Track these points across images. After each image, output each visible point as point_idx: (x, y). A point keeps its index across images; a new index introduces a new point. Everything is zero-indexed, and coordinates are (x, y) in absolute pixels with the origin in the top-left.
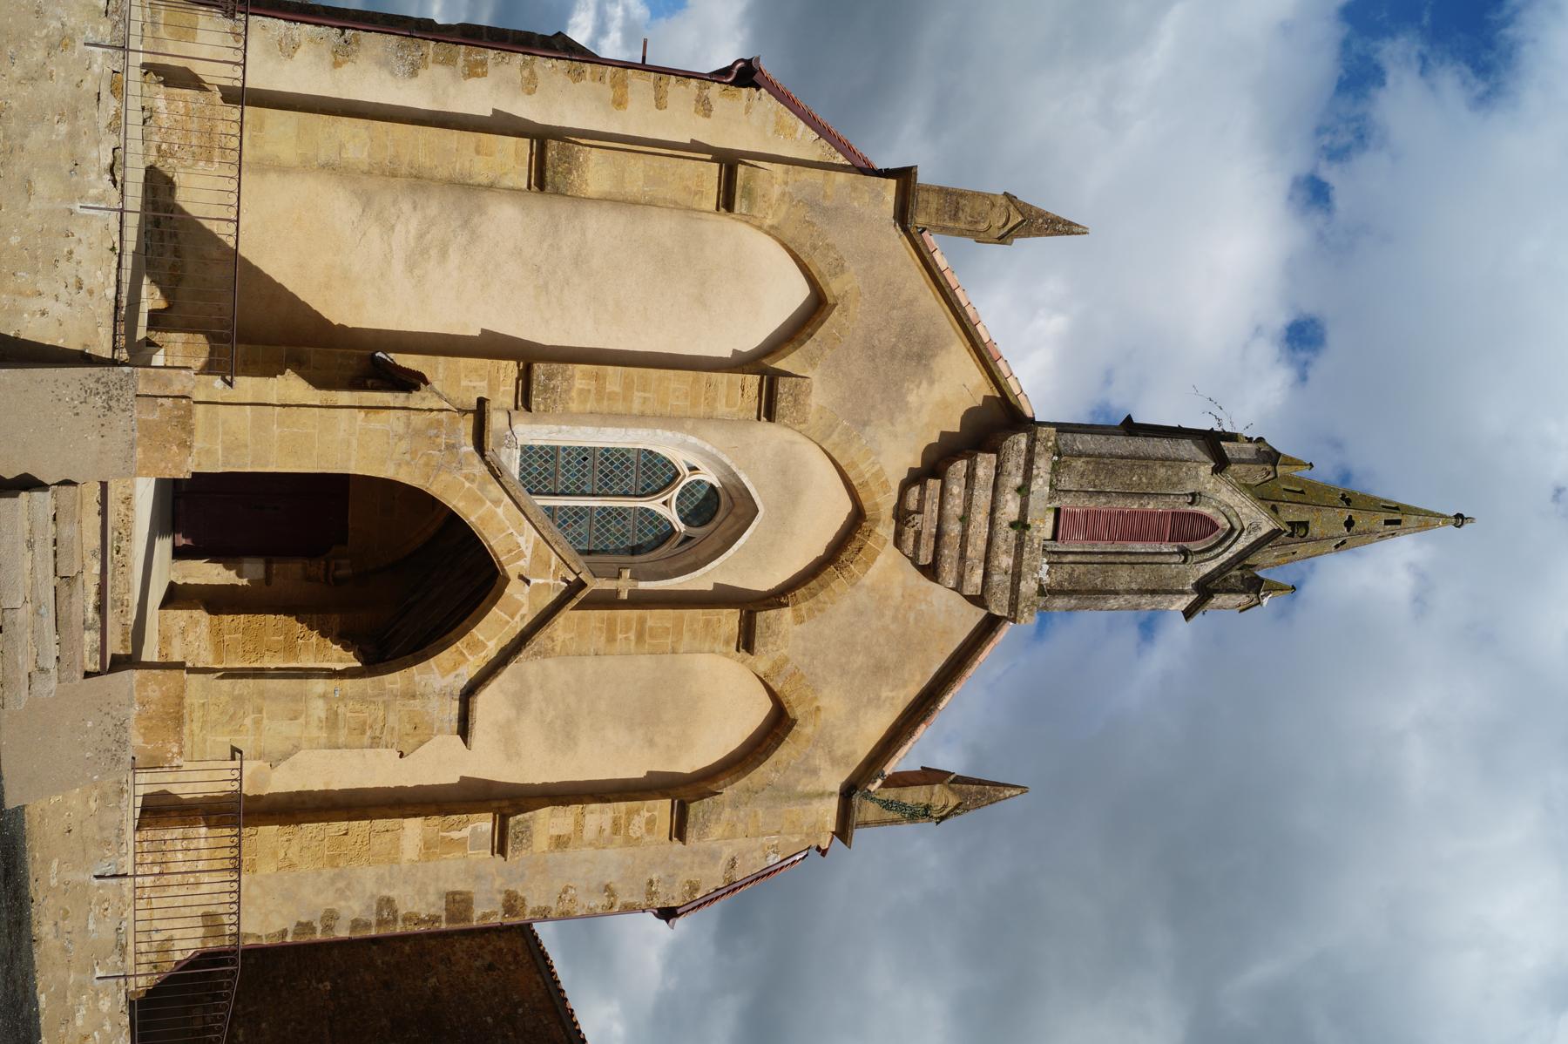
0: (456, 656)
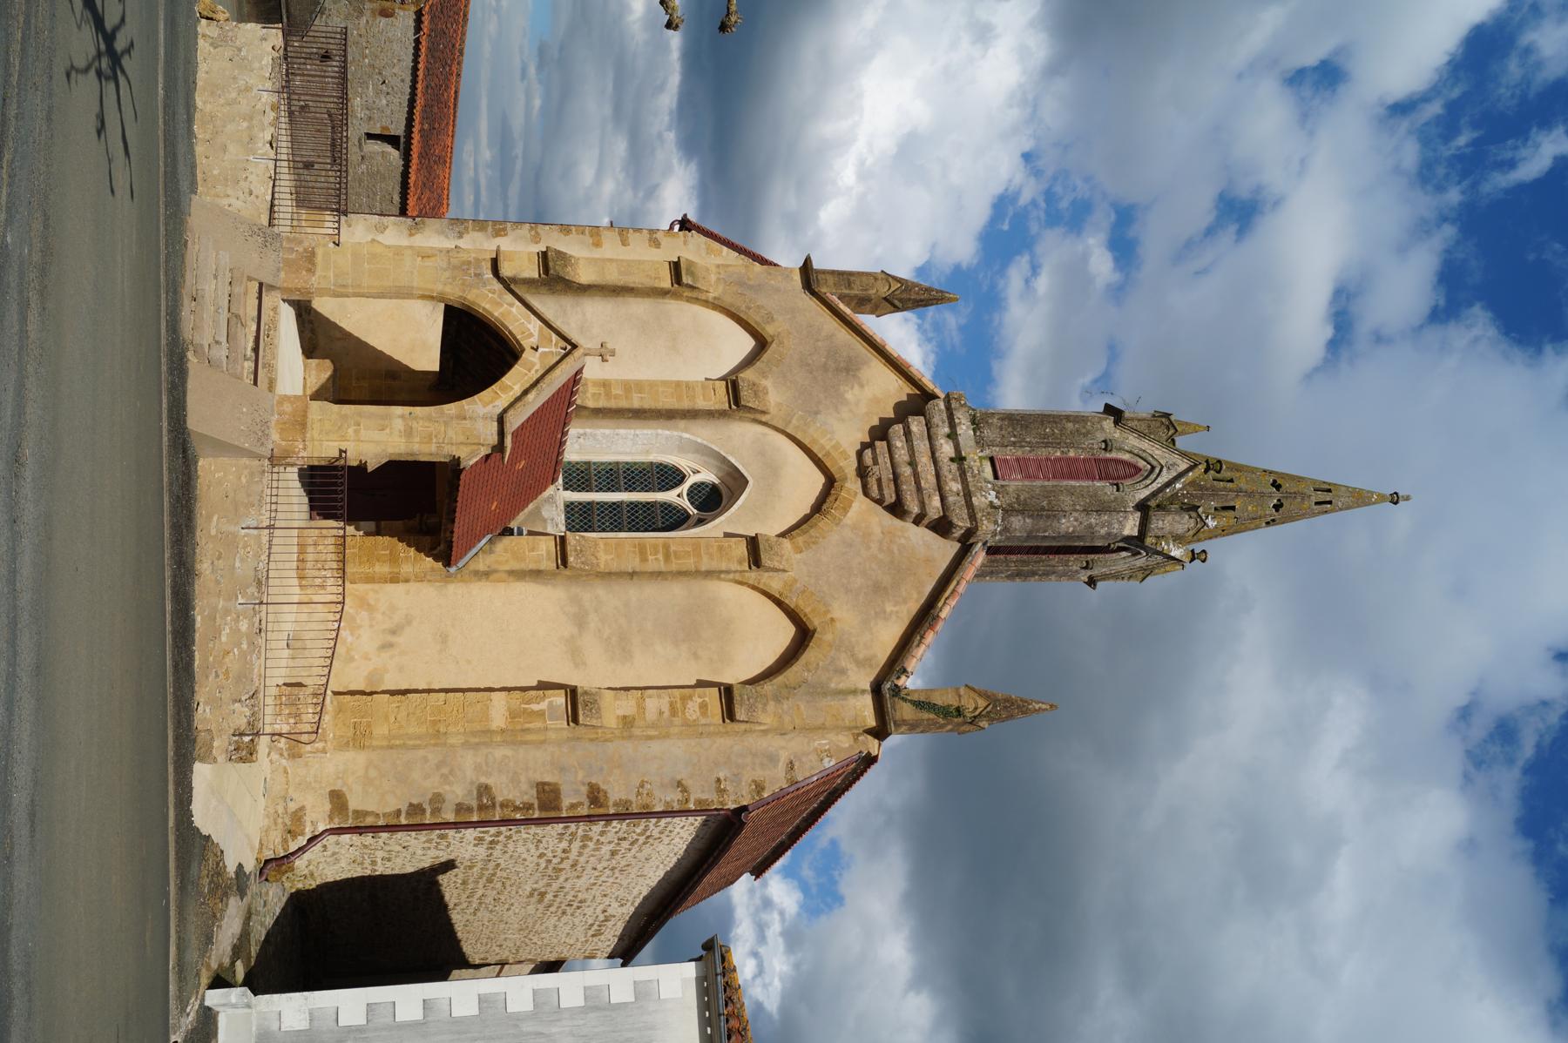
0: (492, 394)
